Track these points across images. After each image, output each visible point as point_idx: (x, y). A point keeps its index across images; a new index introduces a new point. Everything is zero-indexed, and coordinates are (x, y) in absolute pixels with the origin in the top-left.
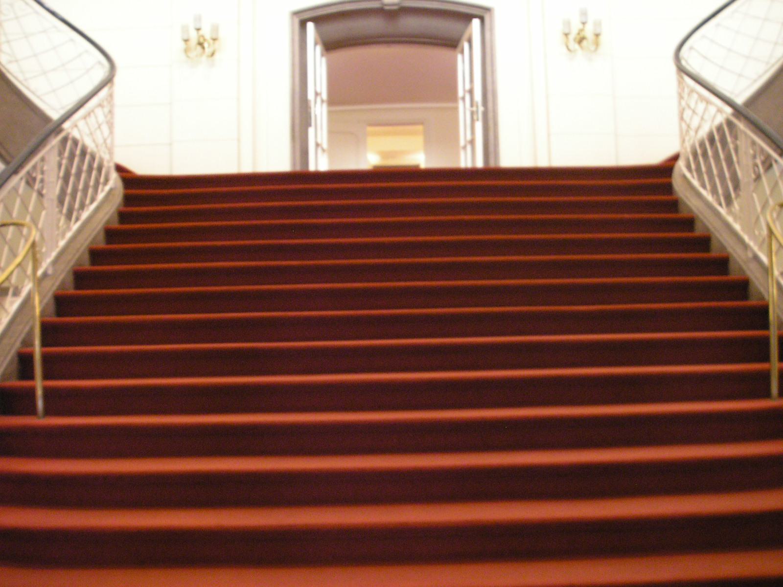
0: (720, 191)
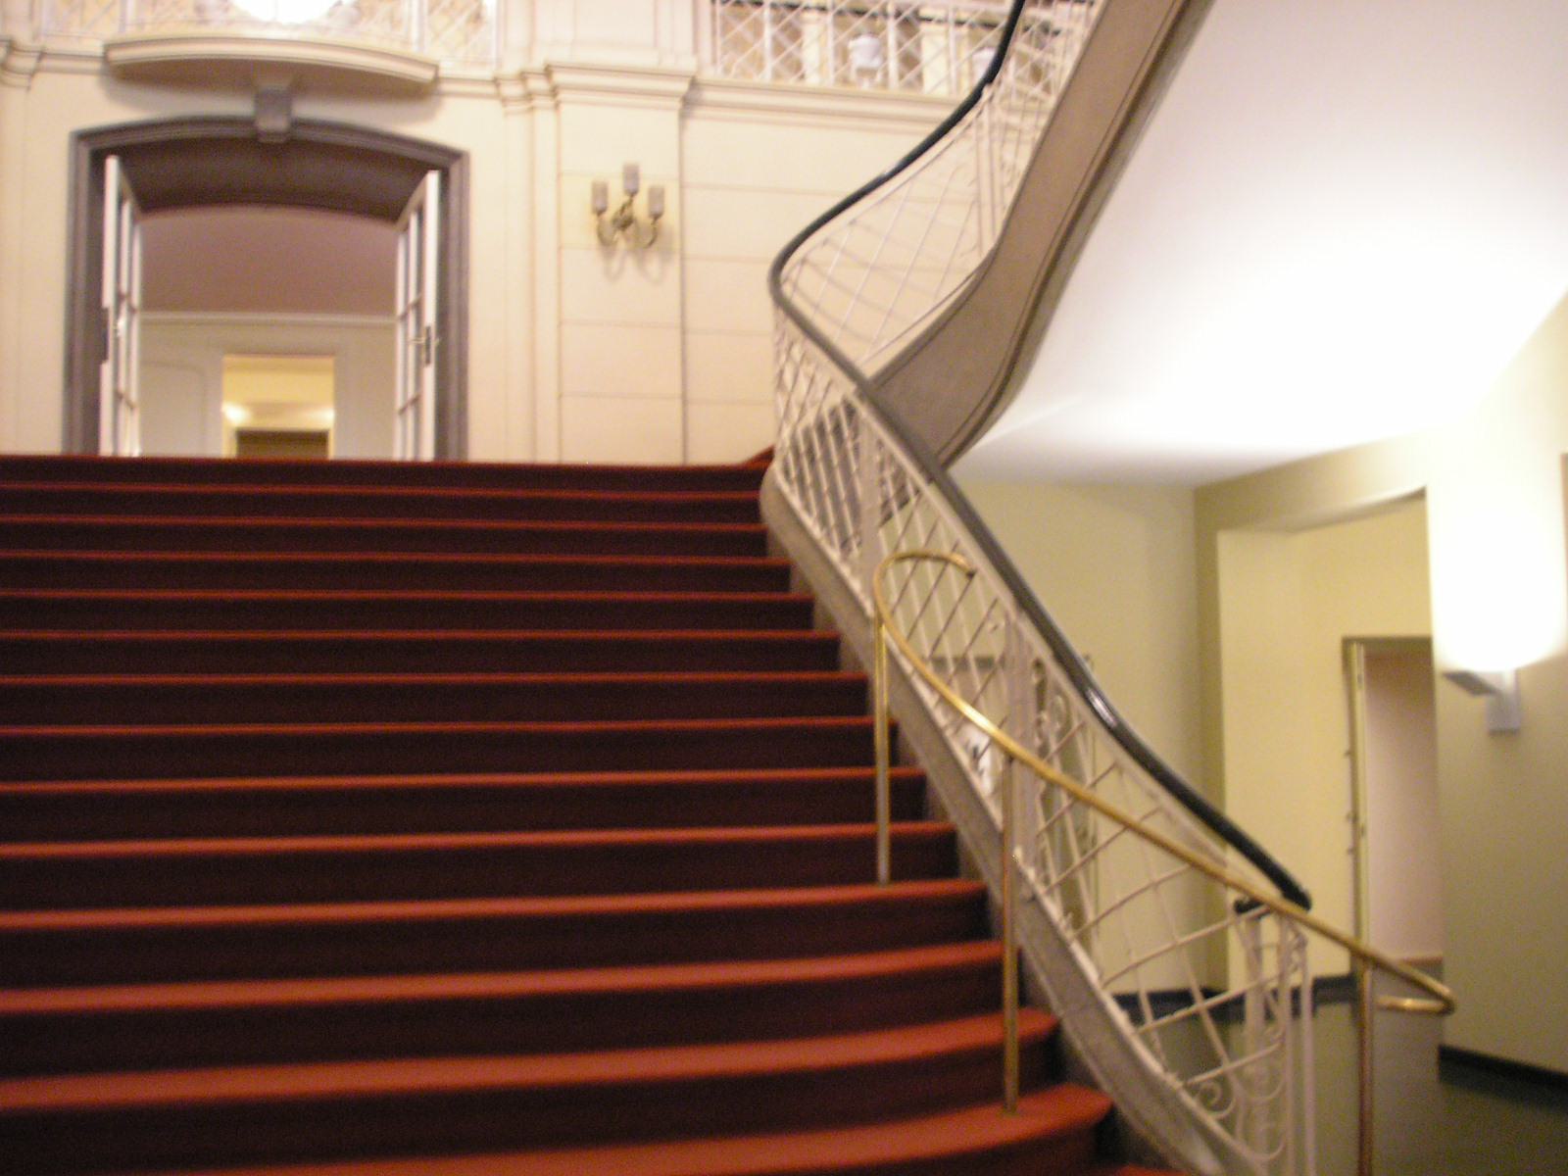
0: (832, 521)
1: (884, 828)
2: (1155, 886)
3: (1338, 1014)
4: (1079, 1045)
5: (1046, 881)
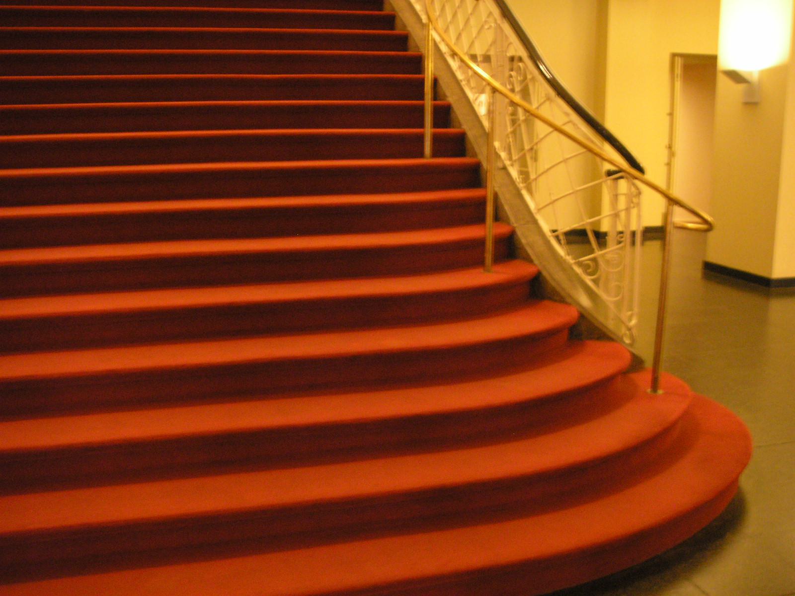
1: (428, 131)
2: (565, 161)
3: (654, 246)
4: (523, 241)
5: (510, 159)
